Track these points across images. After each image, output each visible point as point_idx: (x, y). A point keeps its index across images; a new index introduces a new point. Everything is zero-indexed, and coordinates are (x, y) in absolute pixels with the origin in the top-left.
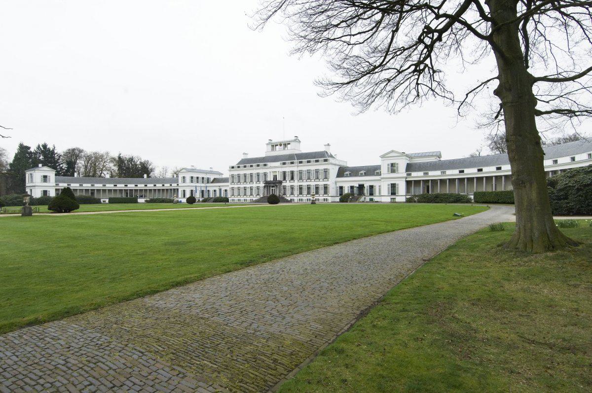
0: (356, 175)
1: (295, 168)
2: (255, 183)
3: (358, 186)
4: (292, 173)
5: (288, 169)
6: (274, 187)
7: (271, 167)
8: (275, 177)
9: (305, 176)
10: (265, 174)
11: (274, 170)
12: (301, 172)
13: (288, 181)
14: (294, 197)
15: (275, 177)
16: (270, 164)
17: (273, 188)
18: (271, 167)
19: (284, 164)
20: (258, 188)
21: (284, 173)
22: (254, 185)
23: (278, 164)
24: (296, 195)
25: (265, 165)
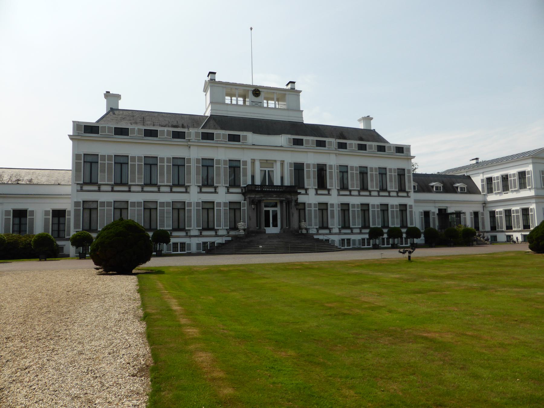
0: (429, 190)
1: (332, 159)
2: (194, 190)
3: (437, 212)
4: (321, 170)
5: (311, 158)
6: (275, 206)
7: (254, 147)
8: (267, 176)
9: (354, 183)
10: (234, 167)
11: (270, 158)
12: (344, 171)
13: (312, 192)
14: (330, 233)
15: (267, 176)
16: (251, 137)
17: (271, 209)
18: (254, 147)
19: (298, 142)
20: (208, 208)
21: (299, 169)
22: (194, 196)
23: (282, 140)
24: (336, 230)
25: (234, 138)
